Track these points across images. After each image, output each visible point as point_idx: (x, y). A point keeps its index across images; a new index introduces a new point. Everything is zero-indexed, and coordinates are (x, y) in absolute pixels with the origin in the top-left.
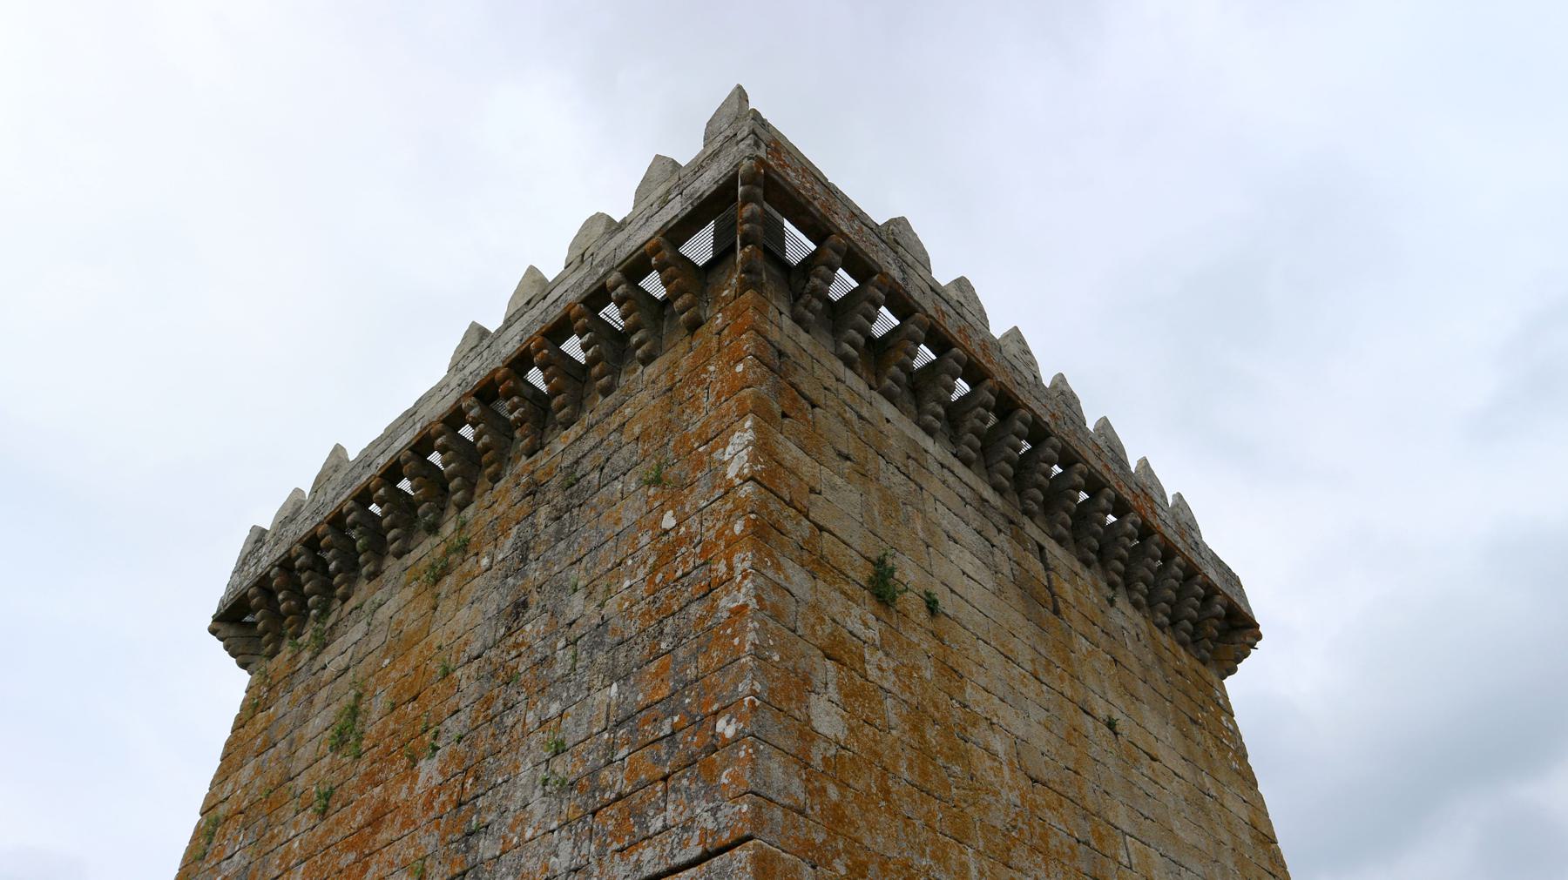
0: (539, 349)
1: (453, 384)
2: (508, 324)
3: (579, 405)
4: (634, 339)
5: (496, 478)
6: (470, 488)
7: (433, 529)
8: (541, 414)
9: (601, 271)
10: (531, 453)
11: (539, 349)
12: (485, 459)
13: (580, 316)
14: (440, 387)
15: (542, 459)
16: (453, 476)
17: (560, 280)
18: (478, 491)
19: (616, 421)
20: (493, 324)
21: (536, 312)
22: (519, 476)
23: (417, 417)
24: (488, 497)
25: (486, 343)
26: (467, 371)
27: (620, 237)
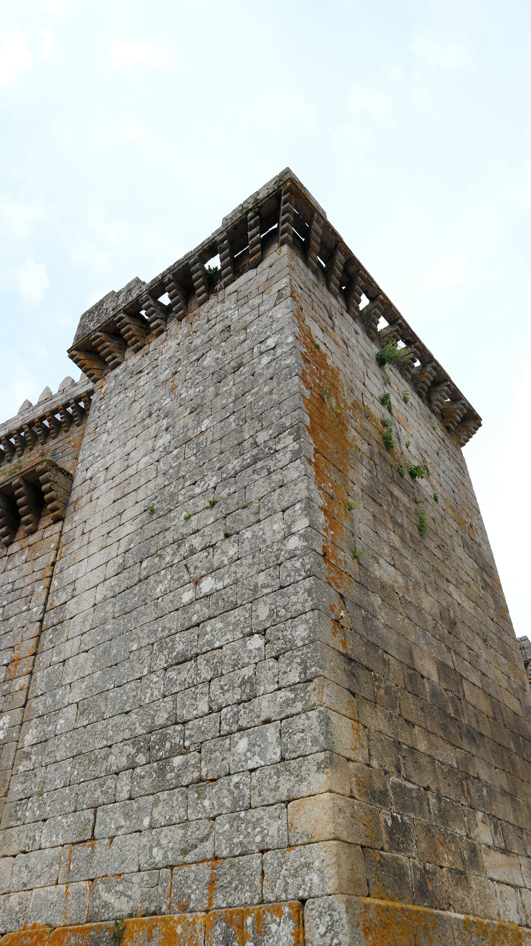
0: (48, 416)
1: (20, 418)
2: (39, 404)
3: (58, 433)
4: (75, 419)
5: (31, 449)
6: (23, 450)
7: (10, 461)
8: (47, 433)
9: (69, 398)
10: (43, 444)
11: (48, 416)
12: (28, 443)
13: (61, 409)
14: (15, 419)
15: (46, 446)
16: (18, 447)
17: (56, 396)
18: (25, 452)
19: (68, 440)
20: (34, 403)
21: (48, 403)
22: (38, 450)
23: (7, 427)
24: (28, 455)
25: (31, 408)
26: (25, 416)
27: (75, 388)
